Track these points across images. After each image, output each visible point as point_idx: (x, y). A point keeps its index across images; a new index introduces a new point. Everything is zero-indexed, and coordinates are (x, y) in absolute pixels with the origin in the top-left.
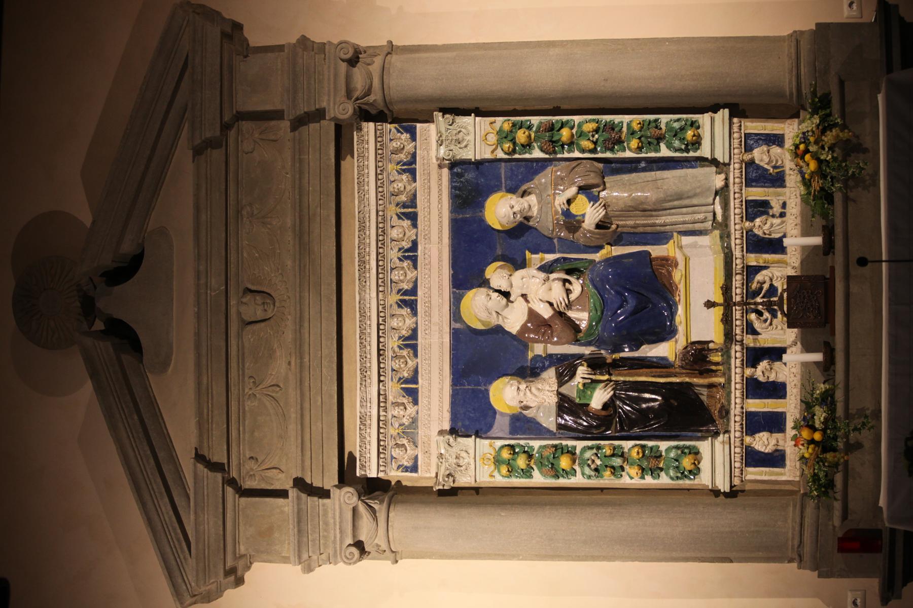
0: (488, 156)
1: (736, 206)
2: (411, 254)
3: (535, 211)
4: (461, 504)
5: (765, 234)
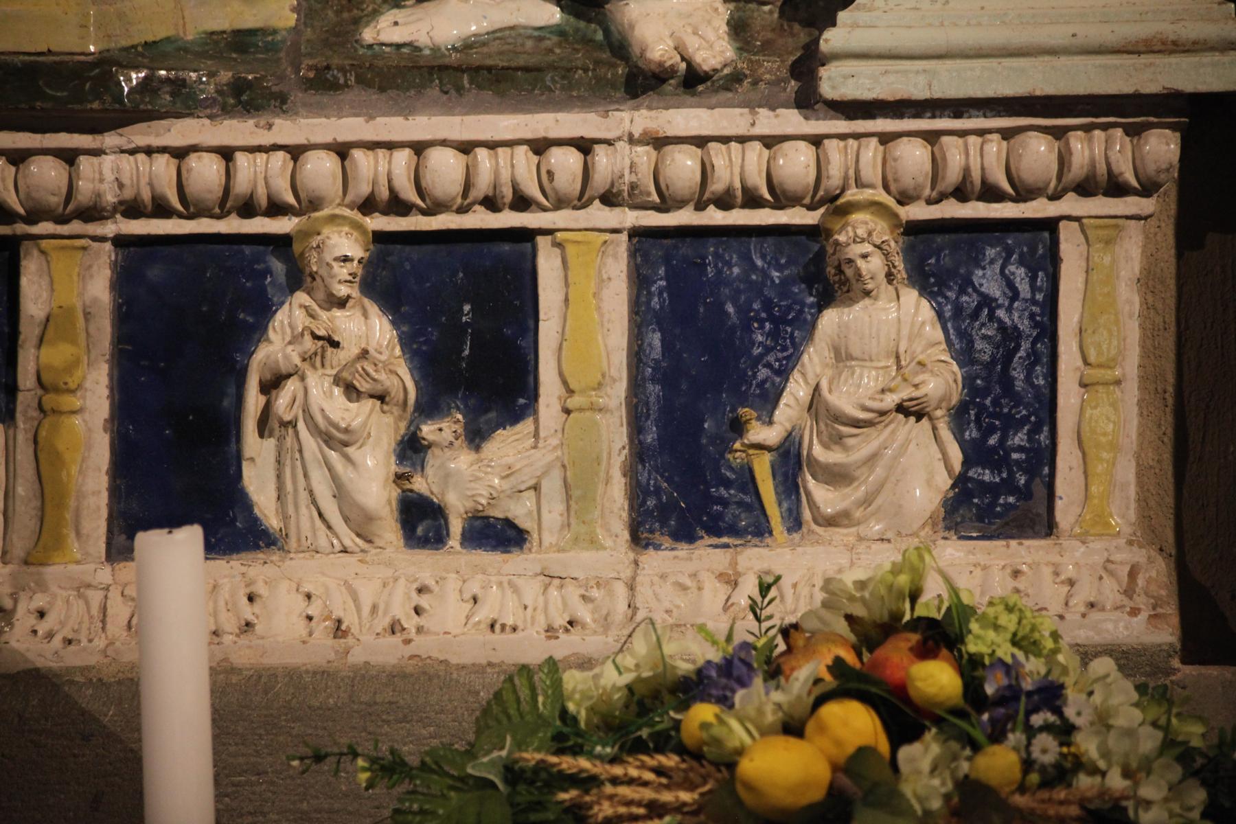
1: (482, 154)
5: (271, 385)
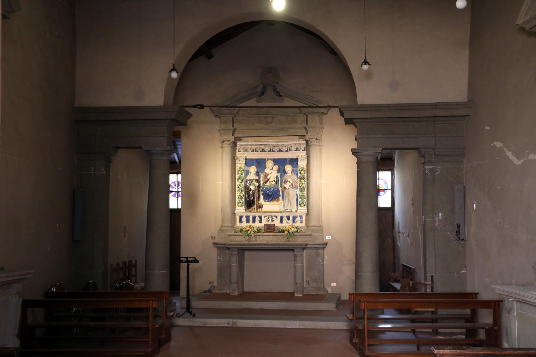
0: (299, 166)
3: (288, 175)
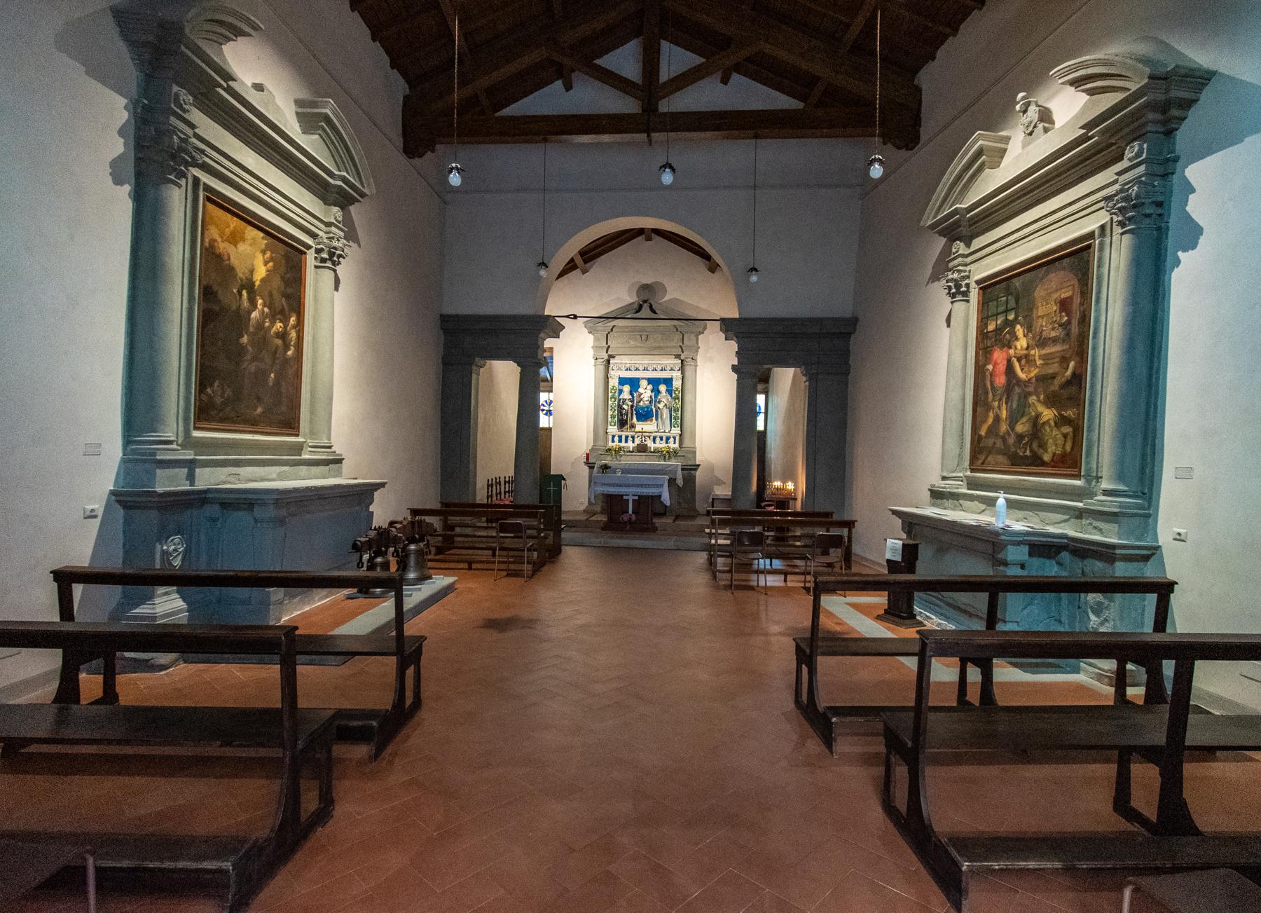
2: (655, 370)
4: (605, 379)
